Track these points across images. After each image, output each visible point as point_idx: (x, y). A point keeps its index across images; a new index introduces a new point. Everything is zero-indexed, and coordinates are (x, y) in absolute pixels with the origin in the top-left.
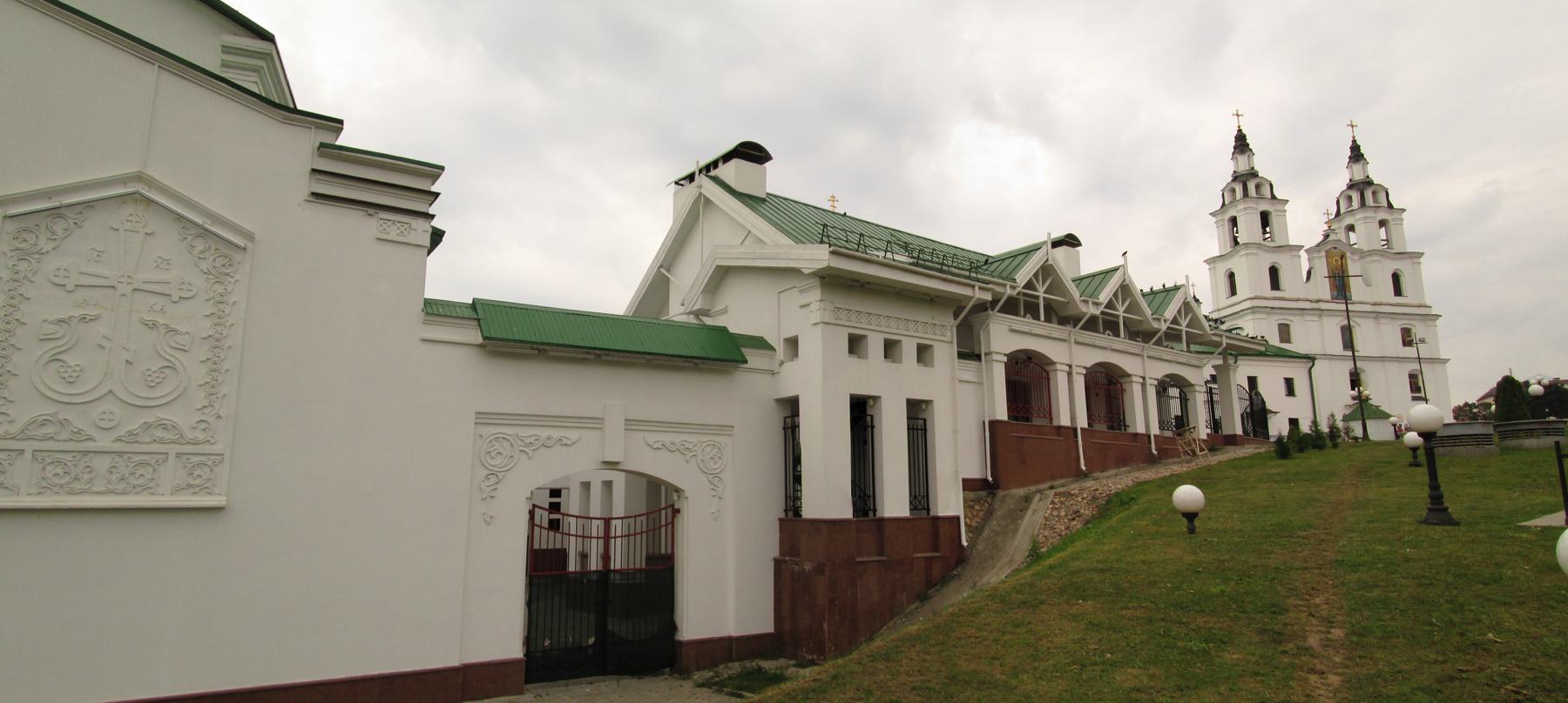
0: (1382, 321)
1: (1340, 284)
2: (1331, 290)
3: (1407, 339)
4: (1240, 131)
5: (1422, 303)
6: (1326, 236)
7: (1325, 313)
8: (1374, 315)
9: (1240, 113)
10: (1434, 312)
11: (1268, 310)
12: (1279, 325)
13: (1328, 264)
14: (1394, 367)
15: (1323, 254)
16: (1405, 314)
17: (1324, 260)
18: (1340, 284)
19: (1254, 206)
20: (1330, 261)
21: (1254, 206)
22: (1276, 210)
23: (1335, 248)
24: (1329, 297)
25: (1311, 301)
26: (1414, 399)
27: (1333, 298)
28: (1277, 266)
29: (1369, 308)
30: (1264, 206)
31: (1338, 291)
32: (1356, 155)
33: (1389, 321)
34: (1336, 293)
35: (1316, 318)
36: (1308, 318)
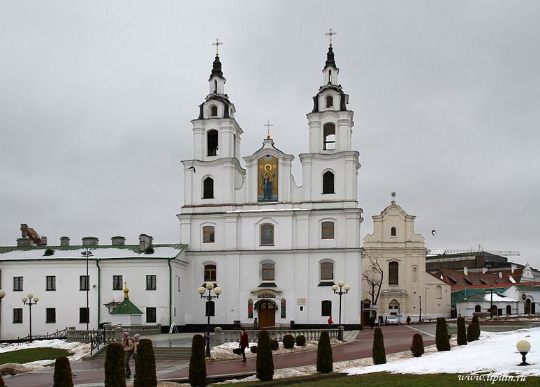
0: (298, 218)
1: (268, 191)
2: (258, 194)
3: (328, 230)
4: (217, 58)
7: (241, 215)
8: (292, 213)
9: (219, 42)
11: (190, 216)
12: (204, 227)
14: (302, 258)
15: (256, 162)
16: (325, 210)
17: (255, 168)
18: (268, 191)
19: (201, 127)
20: (261, 167)
22: (221, 128)
23: (268, 156)
24: (255, 200)
26: (322, 284)
27: (259, 201)
29: (289, 208)
30: (212, 125)
31: (265, 195)
36: (227, 220)
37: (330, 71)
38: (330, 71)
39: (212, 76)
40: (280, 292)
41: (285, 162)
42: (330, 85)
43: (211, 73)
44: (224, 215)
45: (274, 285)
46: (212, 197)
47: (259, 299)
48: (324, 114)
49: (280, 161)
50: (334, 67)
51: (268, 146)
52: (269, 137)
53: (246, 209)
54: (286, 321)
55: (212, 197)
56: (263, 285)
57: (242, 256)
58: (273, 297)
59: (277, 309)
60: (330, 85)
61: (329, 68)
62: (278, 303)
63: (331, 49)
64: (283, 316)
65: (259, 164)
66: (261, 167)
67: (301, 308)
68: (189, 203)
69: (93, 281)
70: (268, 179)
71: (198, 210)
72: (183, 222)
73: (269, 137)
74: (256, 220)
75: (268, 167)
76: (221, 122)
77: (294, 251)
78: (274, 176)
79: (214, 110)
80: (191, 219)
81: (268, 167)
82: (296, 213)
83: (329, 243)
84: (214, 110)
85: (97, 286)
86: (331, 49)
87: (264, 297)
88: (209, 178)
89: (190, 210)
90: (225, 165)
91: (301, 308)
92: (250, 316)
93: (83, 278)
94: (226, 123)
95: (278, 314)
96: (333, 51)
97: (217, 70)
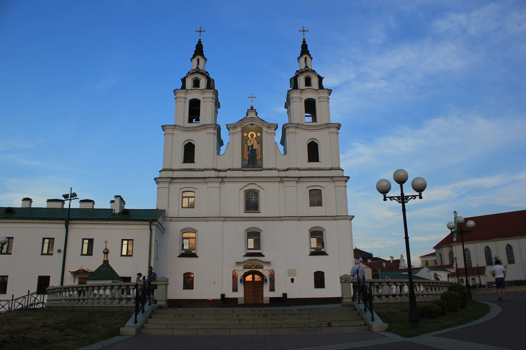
0: (286, 184)
2: (243, 159)
4: (200, 42)
5: (335, 166)
6: (247, 115)
10: (345, 174)
11: (169, 180)
13: (243, 136)
15: (239, 129)
17: (240, 135)
19: (183, 95)
20: (245, 135)
21: (183, 95)
22: (204, 98)
23: (252, 125)
24: (239, 166)
25: (219, 171)
27: (243, 167)
28: (193, 142)
29: (275, 173)
30: (195, 95)
31: (249, 161)
32: (305, 50)
33: (294, 184)
34: (247, 163)
35: (218, 185)
36: (210, 185)
37: (306, 59)
38: (306, 59)
39: (194, 56)
40: (268, 263)
41: (269, 131)
42: (307, 69)
43: (194, 53)
44: (207, 180)
45: (260, 255)
46: (192, 161)
47: (247, 270)
48: (304, 91)
49: (265, 129)
50: (310, 55)
51: (252, 115)
52: (252, 108)
53: (229, 174)
54: (278, 294)
55: (192, 161)
56: (248, 255)
57: (225, 223)
58: (260, 268)
59: (266, 280)
60: (307, 69)
61: (305, 56)
62: (267, 274)
63: (304, 42)
64: (272, 289)
65: (243, 131)
66: (245, 135)
67: (292, 280)
68: (169, 167)
69: (59, 244)
70: (252, 146)
71: (176, 174)
72: (161, 185)
73: (252, 108)
74: (241, 185)
75: (252, 136)
76: (204, 92)
77: (280, 218)
78: (258, 144)
79: (196, 83)
80: (170, 183)
81: (252, 136)
82: (283, 179)
83: (316, 211)
84: (196, 83)
85: (62, 249)
86: (304, 42)
87: (250, 268)
88: (190, 143)
89: (170, 174)
90: (208, 131)
91: (292, 280)
92: (235, 289)
93: (47, 241)
94: (210, 94)
95: (266, 287)
96: (306, 43)
97: (199, 50)
